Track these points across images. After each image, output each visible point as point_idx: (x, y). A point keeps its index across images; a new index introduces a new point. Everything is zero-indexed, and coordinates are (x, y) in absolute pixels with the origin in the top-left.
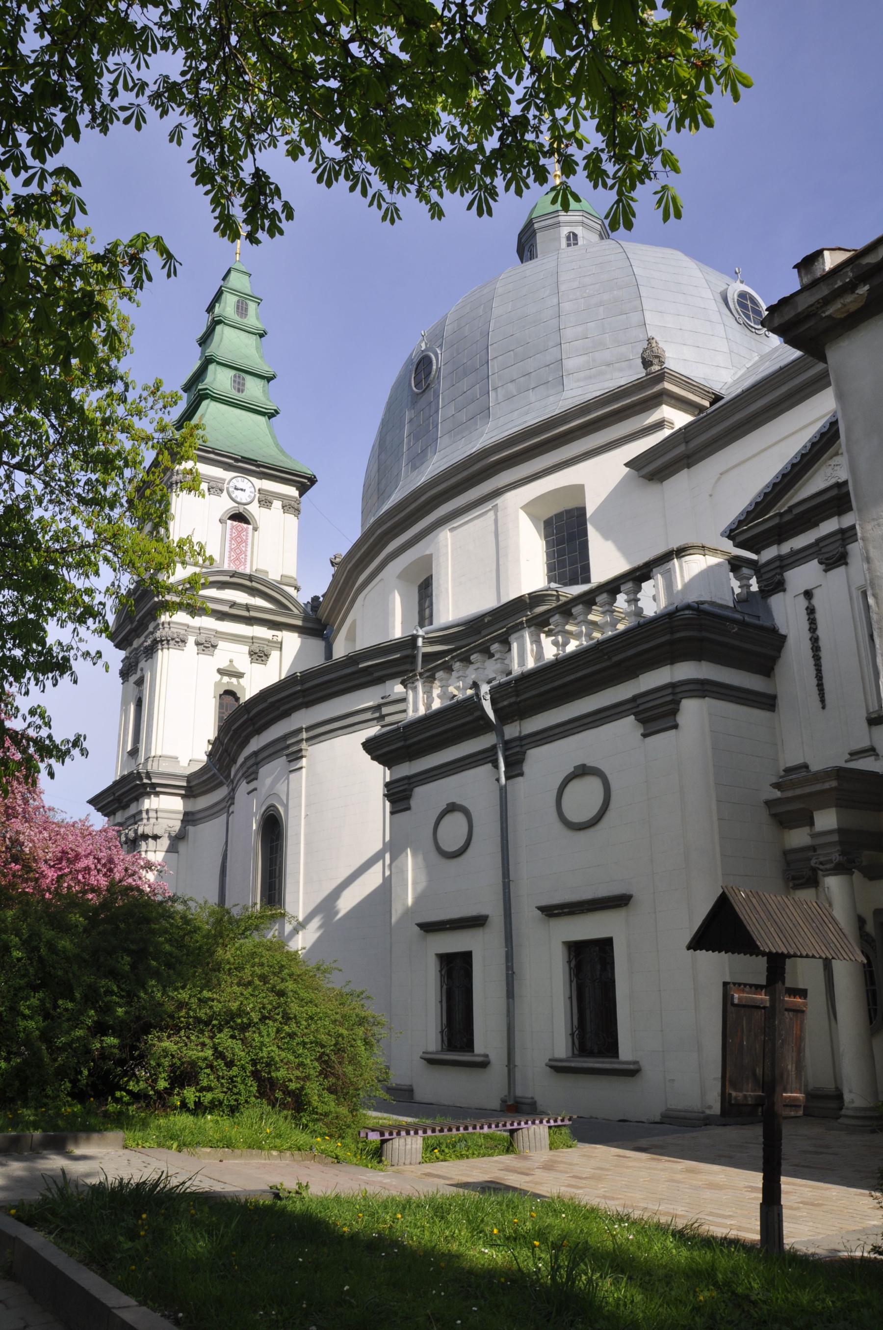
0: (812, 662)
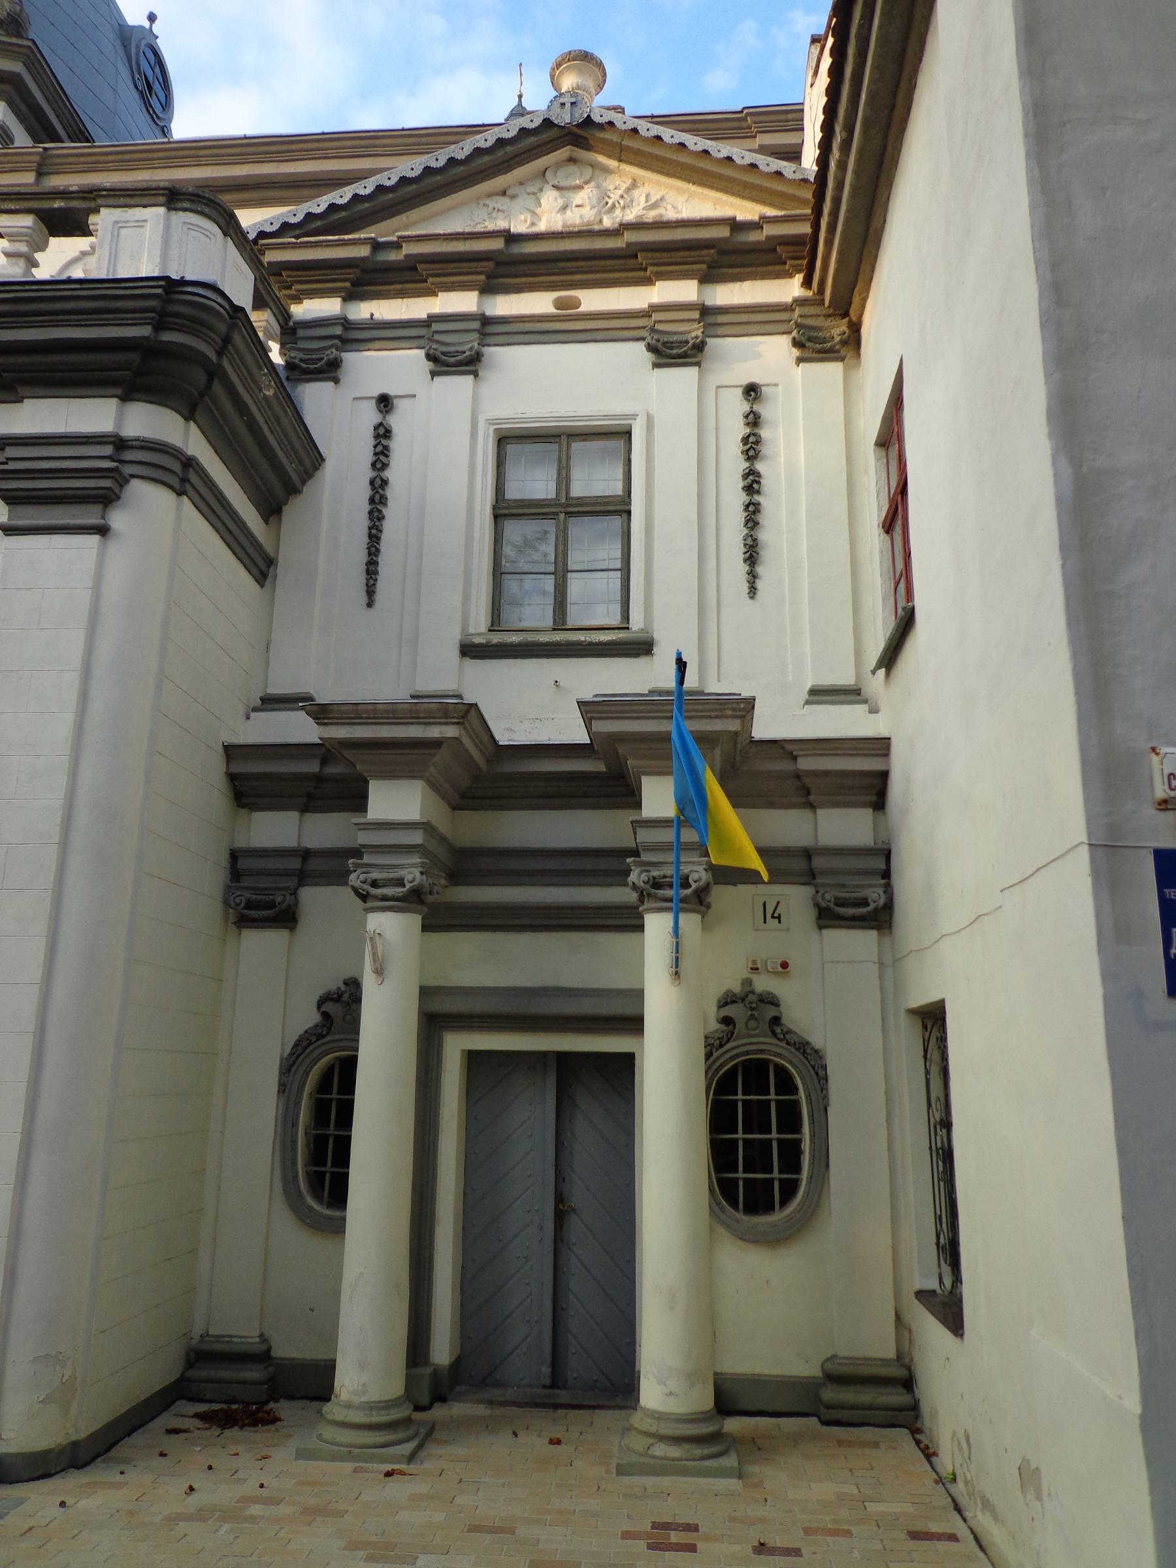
0: (363, 522)
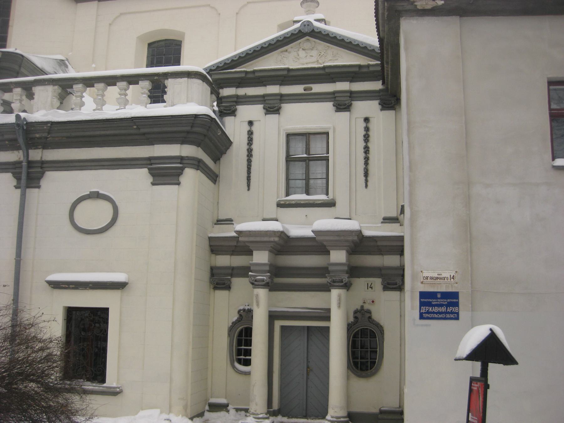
0: (245, 163)
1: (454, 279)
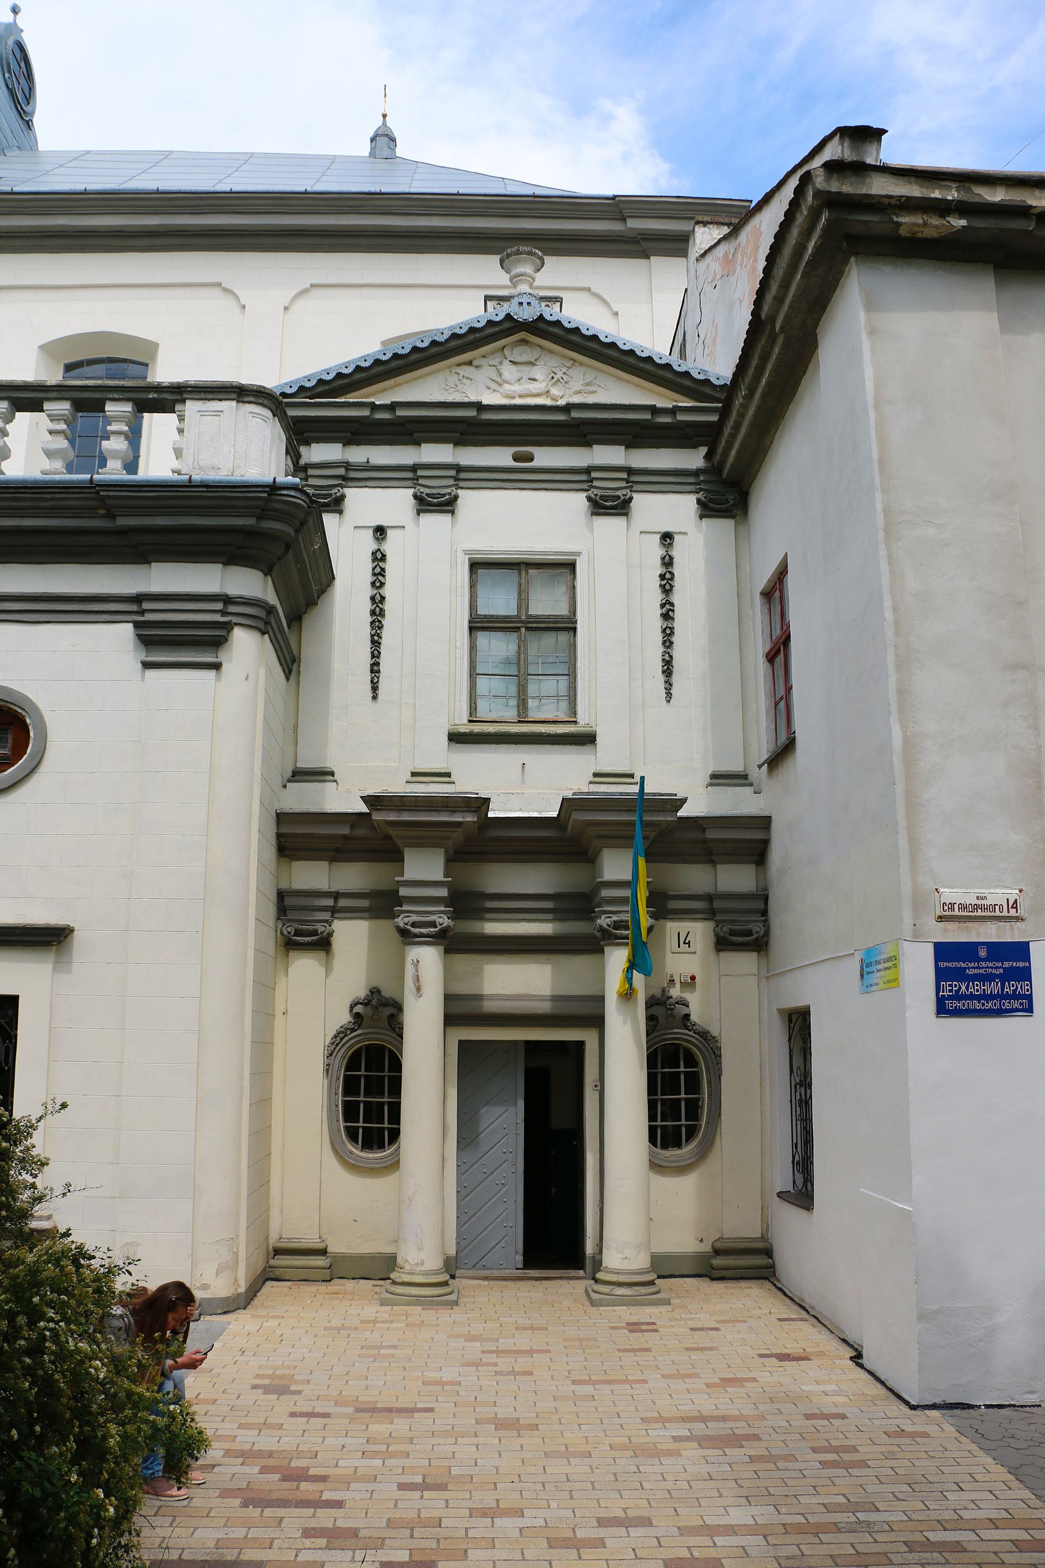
0: (366, 631)
1: (1016, 908)
